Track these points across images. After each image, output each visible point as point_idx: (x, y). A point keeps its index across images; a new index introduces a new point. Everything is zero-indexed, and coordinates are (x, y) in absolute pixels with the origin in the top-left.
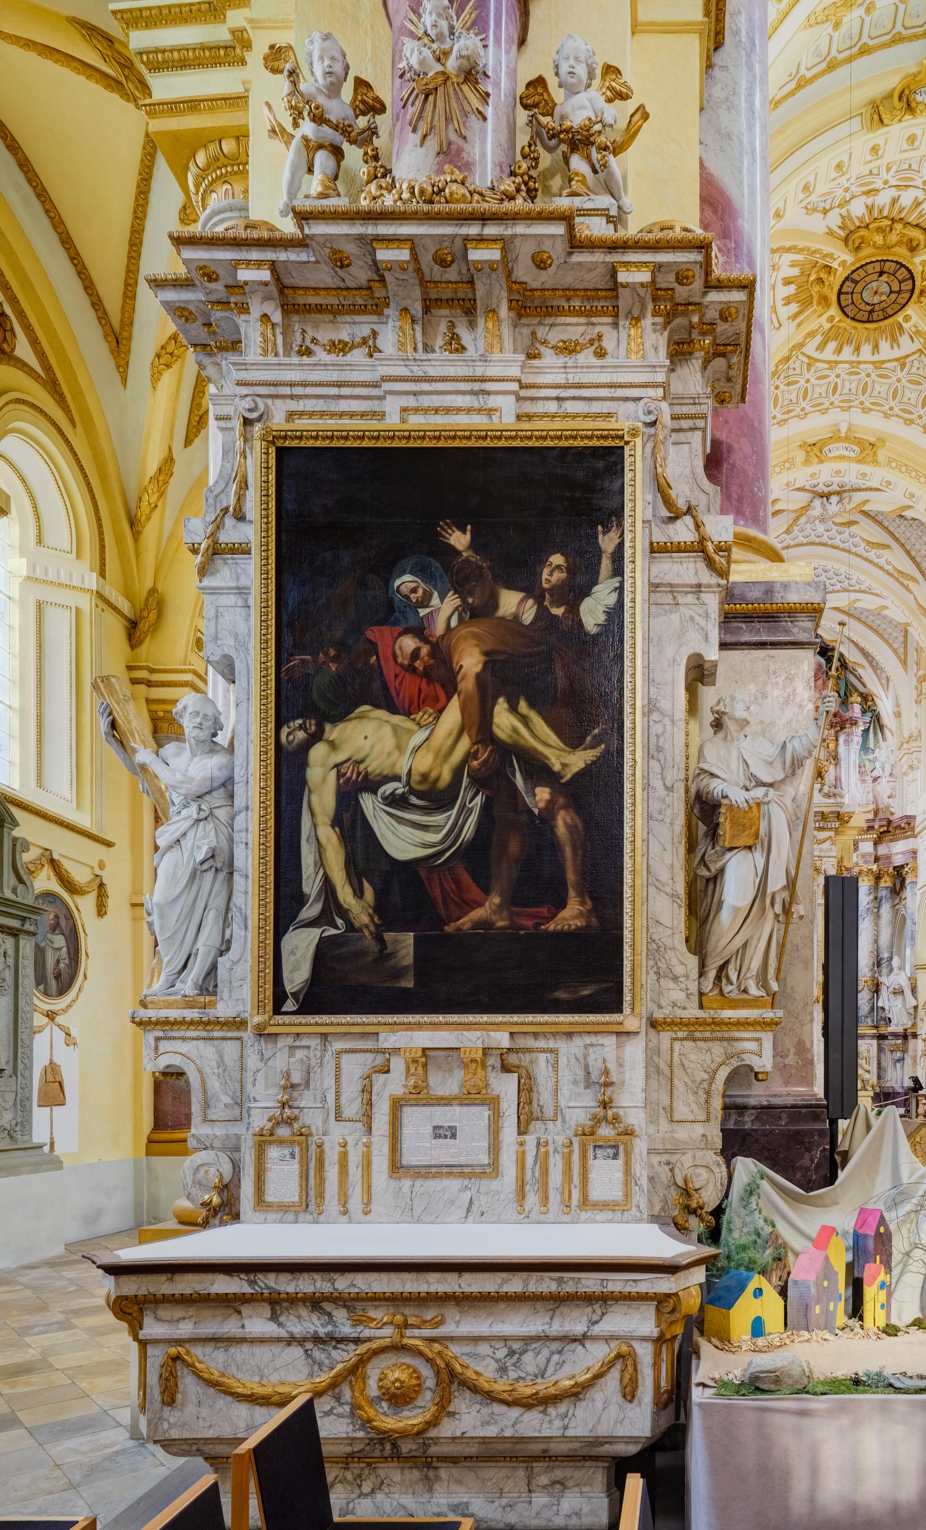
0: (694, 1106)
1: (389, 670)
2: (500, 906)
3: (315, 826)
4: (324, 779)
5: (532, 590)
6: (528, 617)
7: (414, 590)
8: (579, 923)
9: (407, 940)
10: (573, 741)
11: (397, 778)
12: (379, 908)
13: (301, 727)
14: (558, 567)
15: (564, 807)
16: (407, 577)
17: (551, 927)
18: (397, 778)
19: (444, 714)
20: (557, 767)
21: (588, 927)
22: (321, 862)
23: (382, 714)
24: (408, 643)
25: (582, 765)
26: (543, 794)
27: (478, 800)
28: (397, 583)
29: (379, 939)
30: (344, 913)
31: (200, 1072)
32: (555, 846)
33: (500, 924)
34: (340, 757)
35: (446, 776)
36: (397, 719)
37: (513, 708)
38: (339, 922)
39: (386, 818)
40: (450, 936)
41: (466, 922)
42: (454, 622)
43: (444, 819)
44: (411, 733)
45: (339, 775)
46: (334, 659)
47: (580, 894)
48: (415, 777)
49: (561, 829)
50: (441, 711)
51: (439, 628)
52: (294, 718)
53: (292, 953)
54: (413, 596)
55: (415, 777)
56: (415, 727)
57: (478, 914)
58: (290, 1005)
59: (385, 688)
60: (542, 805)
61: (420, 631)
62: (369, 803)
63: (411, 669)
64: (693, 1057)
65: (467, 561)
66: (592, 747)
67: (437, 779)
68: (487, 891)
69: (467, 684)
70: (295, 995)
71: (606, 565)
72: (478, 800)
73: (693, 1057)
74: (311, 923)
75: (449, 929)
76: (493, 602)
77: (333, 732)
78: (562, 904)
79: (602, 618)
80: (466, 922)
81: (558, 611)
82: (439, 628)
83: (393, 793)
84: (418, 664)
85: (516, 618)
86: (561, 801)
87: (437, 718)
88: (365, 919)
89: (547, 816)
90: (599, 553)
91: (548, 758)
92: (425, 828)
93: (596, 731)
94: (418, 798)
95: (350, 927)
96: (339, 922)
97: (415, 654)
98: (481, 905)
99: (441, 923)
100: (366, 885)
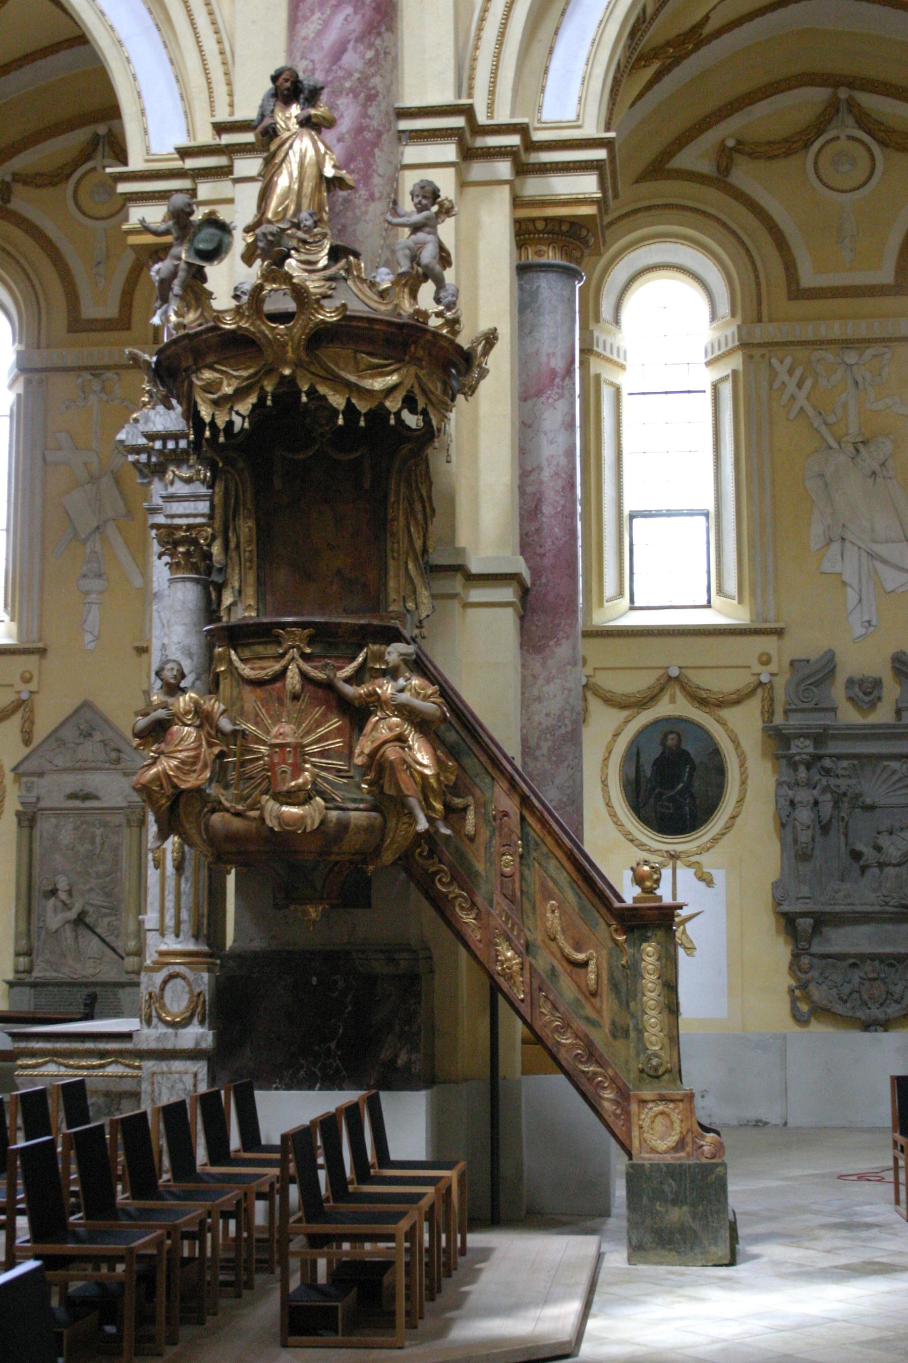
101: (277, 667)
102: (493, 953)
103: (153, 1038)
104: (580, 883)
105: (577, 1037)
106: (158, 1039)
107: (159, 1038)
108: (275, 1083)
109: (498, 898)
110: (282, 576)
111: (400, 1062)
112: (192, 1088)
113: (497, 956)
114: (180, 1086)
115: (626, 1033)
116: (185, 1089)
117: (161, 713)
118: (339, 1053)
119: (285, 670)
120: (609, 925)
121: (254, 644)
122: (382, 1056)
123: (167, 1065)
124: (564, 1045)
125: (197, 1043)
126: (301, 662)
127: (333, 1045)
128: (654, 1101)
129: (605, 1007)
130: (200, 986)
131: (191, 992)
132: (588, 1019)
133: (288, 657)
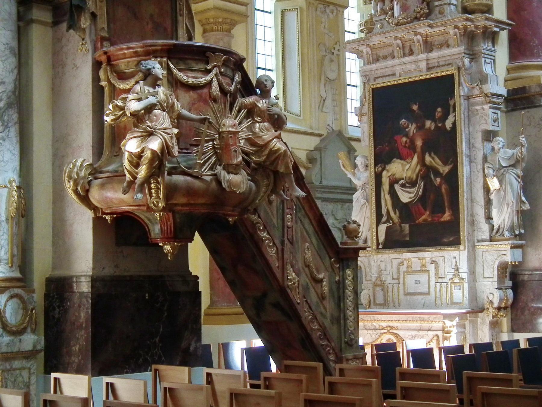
0: (490, 273)
1: (400, 147)
2: (429, 215)
3: (384, 195)
4: (386, 181)
5: (433, 119)
6: (433, 128)
7: (405, 124)
8: (449, 218)
9: (407, 225)
10: (445, 163)
11: (403, 179)
12: (400, 217)
13: (380, 167)
14: (440, 112)
15: (443, 183)
16: (403, 120)
17: (442, 220)
18: (403, 179)
19: (414, 159)
20: (441, 172)
21: (451, 219)
22: (386, 205)
23: (399, 161)
24: (404, 139)
25: (448, 170)
26: (438, 180)
27: (423, 183)
28: (401, 122)
29: (400, 226)
30: (392, 219)
31: (365, 266)
32: (442, 195)
33: (429, 220)
34: (389, 174)
35: (414, 177)
36: (402, 162)
37: (430, 155)
38: (391, 222)
39: (401, 190)
40: (417, 224)
41: (421, 220)
42: (415, 132)
43: (415, 190)
44: (406, 165)
45: (390, 179)
46: (387, 146)
47: (449, 209)
48: (407, 178)
49: (443, 190)
50: (412, 158)
51: (411, 134)
52: (379, 164)
53: (380, 231)
54: (405, 125)
55: (407, 178)
56: (407, 164)
57: (424, 217)
58: (380, 247)
59: (399, 153)
60: (438, 183)
61: (407, 135)
62: (397, 187)
63: (405, 147)
64: (488, 257)
65: (417, 113)
66: (450, 164)
67: (412, 179)
68: (426, 210)
69: (419, 149)
70: (381, 243)
71: (451, 109)
72: (423, 183)
73: (488, 257)
74: (384, 223)
75: (417, 222)
76: (424, 125)
77: (388, 167)
78: (444, 213)
79: (451, 126)
80: (421, 220)
81: (440, 125)
82: (411, 134)
83: (402, 183)
84: (407, 145)
85: (430, 128)
86: (443, 182)
87: (412, 160)
88: (397, 220)
89: (440, 187)
90: (449, 105)
91: (439, 169)
92: (410, 193)
93: (451, 160)
94: (409, 184)
95: (394, 223)
96: (391, 222)
97: (406, 142)
98: (424, 214)
99: (415, 220)
100: (397, 211)
101: (208, 78)
102: (286, 275)
103: (4, 344)
104: (319, 233)
105: (320, 326)
106: (8, 345)
107: (8, 344)
108: (126, 368)
109: (286, 241)
110: (120, 12)
111: (192, 348)
112: (28, 380)
113: (288, 277)
114: (20, 379)
115: (338, 321)
116: (24, 381)
117: (152, 100)
118: (160, 345)
119: (211, 81)
120: (331, 258)
121: (187, 59)
122: (183, 345)
123: (9, 365)
124: (314, 330)
125: (34, 346)
126: (220, 77)
127: (157, 339)
128: (351, 359)
129: (328, 306)
130: (31, 303)
131: (25, 308)
132: (322, 313)
133: (214, 72)
